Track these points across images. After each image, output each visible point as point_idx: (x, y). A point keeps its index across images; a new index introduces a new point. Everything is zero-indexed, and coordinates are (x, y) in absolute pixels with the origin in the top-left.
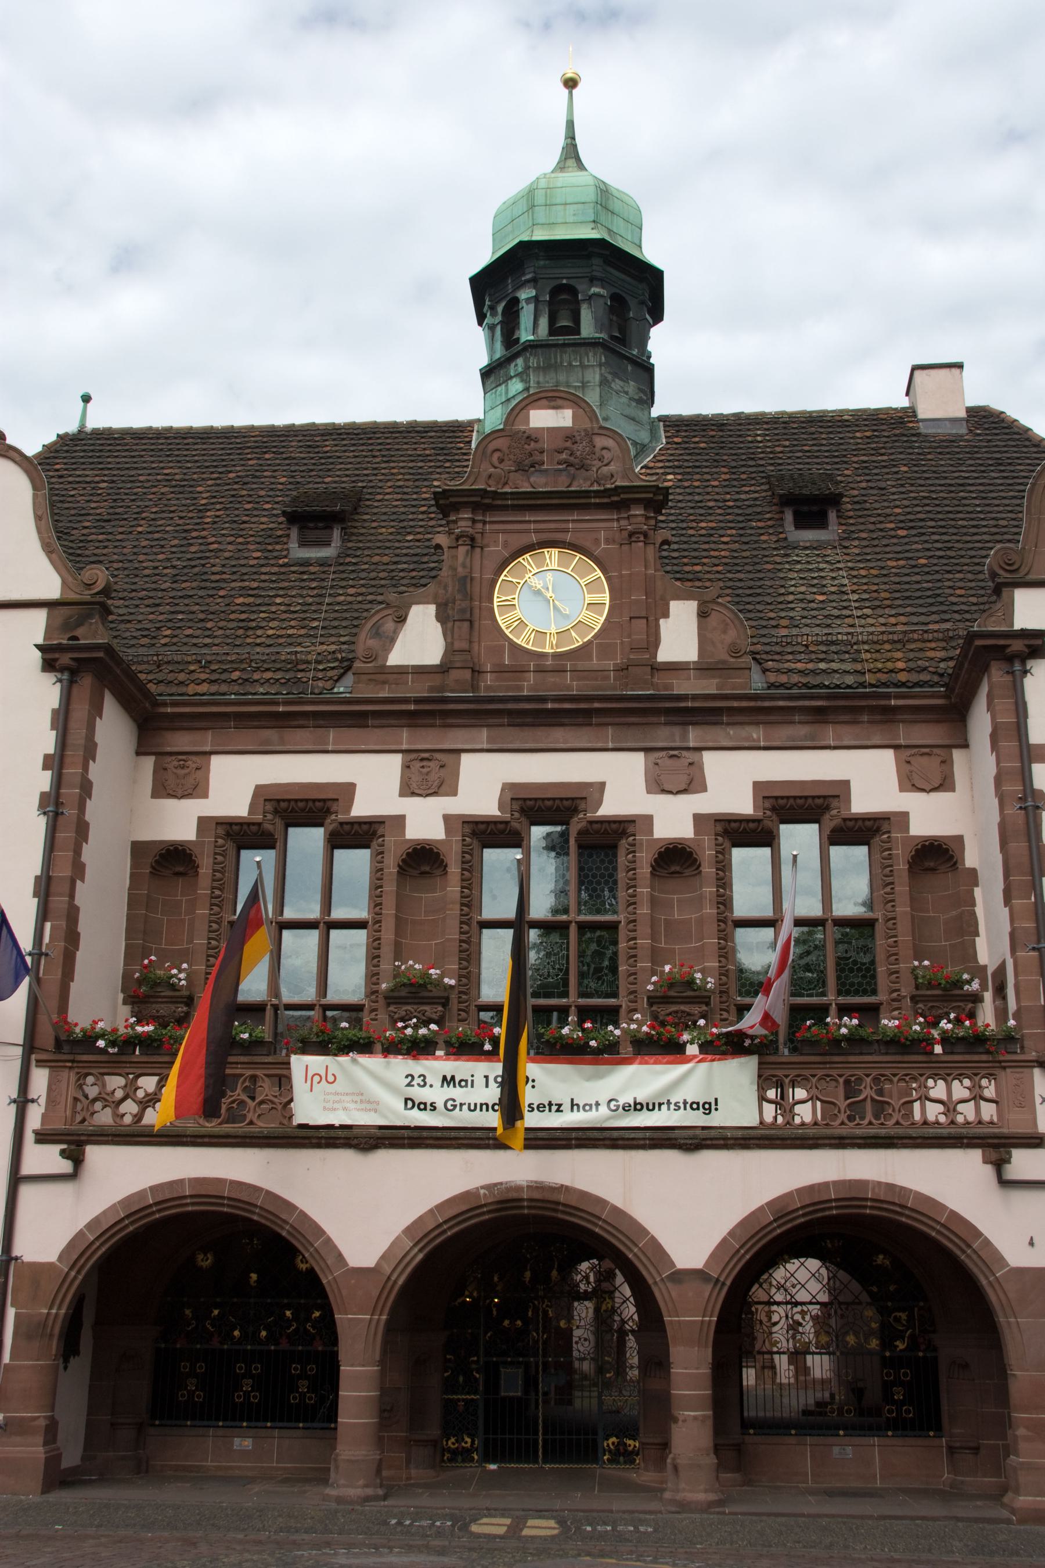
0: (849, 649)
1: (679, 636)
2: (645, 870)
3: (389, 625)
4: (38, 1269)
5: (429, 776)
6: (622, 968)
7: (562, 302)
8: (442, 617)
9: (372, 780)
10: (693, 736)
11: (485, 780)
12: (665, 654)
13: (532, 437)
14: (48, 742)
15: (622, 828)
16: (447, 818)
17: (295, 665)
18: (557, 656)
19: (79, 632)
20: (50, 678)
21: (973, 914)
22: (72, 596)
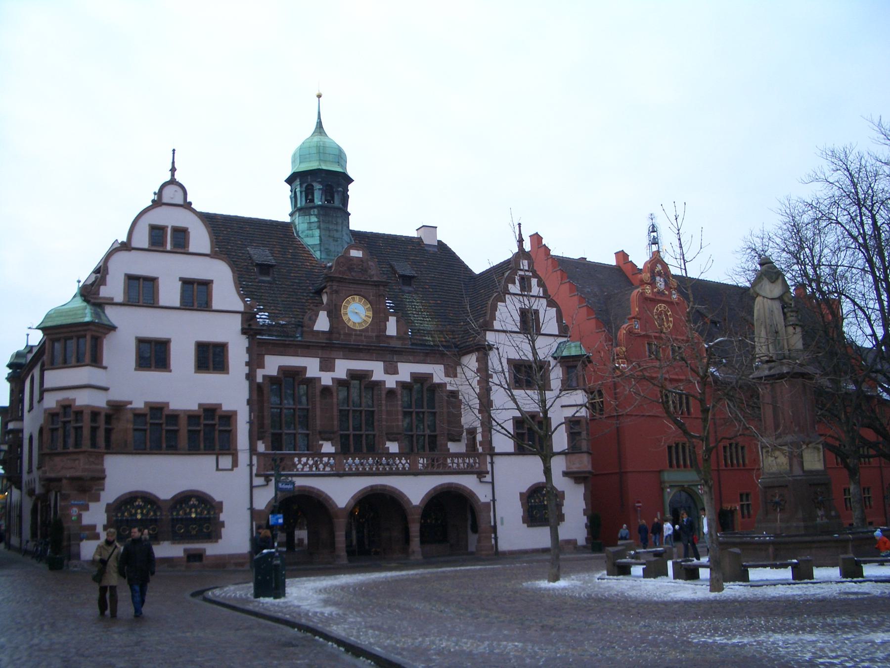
0: (429, 333)
1: (392, 328)
2: (384, 396)
4: (260, 511)
5: (327, 366)
6: (375, 424)
7: (329, 193)
8: (329, 316)
9: (312, 366)
10: (395, 358)
11: (343, 367)
12: (388, 333)
14: (246, 358)
15: (380, 384)
16: (333, 379)
18: (360, 331)
20: (244, 337)
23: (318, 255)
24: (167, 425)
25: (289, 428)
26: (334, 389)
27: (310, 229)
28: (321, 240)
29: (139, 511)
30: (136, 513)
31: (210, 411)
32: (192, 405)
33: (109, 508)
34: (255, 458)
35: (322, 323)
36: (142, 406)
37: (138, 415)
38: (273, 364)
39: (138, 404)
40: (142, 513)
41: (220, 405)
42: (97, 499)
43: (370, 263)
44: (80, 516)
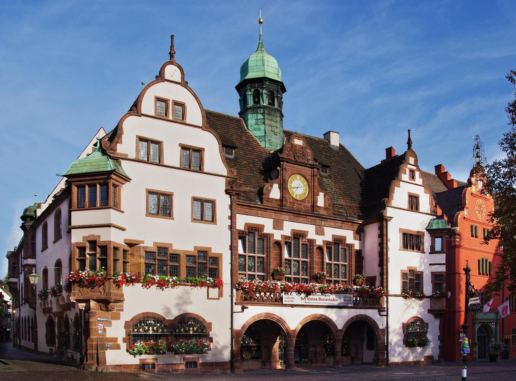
3: (270, 188)
8: (280, 188)
9: (267, 224)
11: (289, 227)
13: (296, 146)
14: (229, 213)
16: (281, 235)
17: (245, 192)
18: (300, 201)
19: (233, 186)
21: (356, 263)
22: (230, 176)
23: (262, 144)
24: (171, 261)
25: (250, 270)
26: (283, 243)
27: (257, 124)
28: (265, 133)
29: (151, 328)
30: (148, 330)
31: (204, 253)
32: (190, 248)
33: (127, 325)
34: (234, 290)
35: (275, 193)
36: (151, 245)
37: (149, 253)
38: (242, 221)
39: (149, 244)
40: (153, 330)
41: (210, 249)
42: (117, 317)
43: (308, 151)
44: (104, 330)
